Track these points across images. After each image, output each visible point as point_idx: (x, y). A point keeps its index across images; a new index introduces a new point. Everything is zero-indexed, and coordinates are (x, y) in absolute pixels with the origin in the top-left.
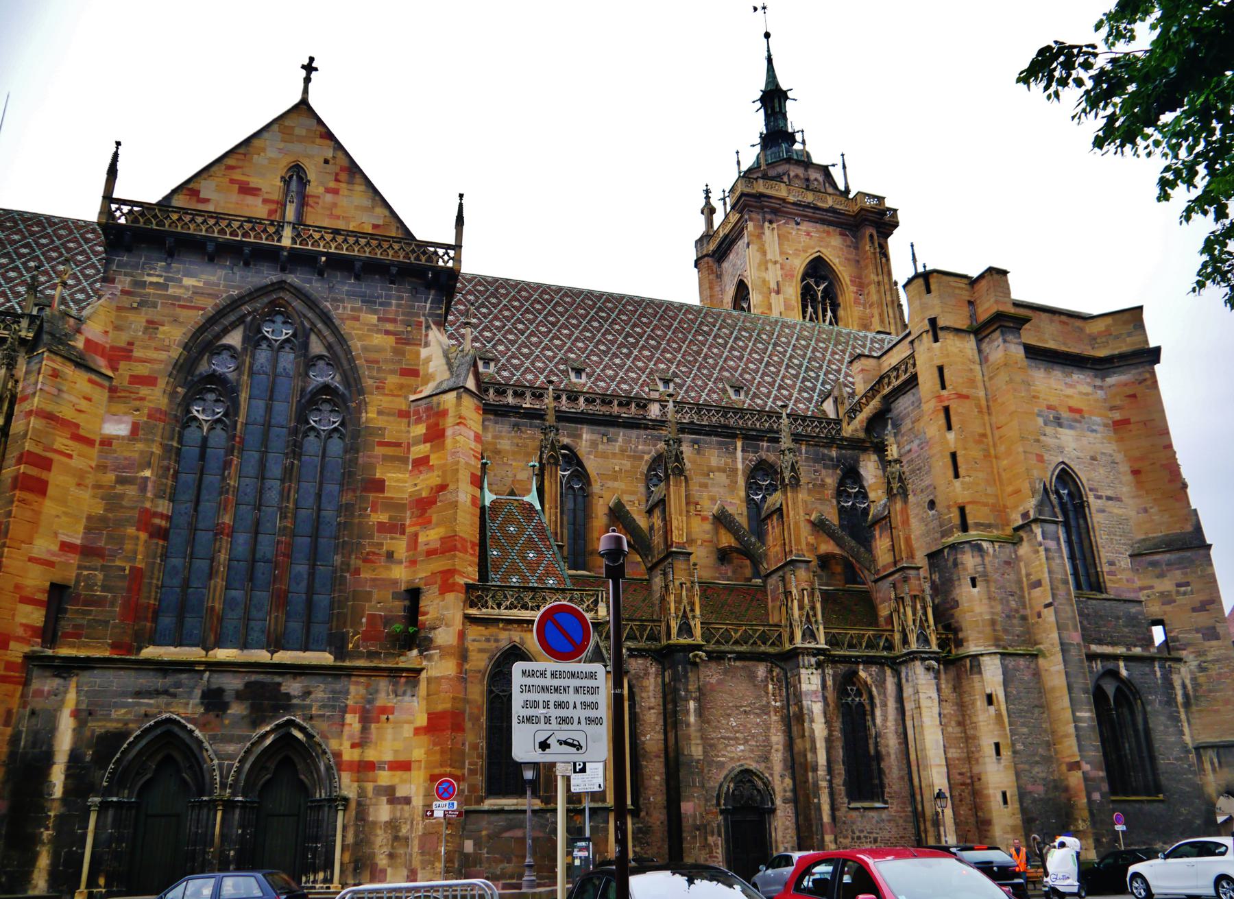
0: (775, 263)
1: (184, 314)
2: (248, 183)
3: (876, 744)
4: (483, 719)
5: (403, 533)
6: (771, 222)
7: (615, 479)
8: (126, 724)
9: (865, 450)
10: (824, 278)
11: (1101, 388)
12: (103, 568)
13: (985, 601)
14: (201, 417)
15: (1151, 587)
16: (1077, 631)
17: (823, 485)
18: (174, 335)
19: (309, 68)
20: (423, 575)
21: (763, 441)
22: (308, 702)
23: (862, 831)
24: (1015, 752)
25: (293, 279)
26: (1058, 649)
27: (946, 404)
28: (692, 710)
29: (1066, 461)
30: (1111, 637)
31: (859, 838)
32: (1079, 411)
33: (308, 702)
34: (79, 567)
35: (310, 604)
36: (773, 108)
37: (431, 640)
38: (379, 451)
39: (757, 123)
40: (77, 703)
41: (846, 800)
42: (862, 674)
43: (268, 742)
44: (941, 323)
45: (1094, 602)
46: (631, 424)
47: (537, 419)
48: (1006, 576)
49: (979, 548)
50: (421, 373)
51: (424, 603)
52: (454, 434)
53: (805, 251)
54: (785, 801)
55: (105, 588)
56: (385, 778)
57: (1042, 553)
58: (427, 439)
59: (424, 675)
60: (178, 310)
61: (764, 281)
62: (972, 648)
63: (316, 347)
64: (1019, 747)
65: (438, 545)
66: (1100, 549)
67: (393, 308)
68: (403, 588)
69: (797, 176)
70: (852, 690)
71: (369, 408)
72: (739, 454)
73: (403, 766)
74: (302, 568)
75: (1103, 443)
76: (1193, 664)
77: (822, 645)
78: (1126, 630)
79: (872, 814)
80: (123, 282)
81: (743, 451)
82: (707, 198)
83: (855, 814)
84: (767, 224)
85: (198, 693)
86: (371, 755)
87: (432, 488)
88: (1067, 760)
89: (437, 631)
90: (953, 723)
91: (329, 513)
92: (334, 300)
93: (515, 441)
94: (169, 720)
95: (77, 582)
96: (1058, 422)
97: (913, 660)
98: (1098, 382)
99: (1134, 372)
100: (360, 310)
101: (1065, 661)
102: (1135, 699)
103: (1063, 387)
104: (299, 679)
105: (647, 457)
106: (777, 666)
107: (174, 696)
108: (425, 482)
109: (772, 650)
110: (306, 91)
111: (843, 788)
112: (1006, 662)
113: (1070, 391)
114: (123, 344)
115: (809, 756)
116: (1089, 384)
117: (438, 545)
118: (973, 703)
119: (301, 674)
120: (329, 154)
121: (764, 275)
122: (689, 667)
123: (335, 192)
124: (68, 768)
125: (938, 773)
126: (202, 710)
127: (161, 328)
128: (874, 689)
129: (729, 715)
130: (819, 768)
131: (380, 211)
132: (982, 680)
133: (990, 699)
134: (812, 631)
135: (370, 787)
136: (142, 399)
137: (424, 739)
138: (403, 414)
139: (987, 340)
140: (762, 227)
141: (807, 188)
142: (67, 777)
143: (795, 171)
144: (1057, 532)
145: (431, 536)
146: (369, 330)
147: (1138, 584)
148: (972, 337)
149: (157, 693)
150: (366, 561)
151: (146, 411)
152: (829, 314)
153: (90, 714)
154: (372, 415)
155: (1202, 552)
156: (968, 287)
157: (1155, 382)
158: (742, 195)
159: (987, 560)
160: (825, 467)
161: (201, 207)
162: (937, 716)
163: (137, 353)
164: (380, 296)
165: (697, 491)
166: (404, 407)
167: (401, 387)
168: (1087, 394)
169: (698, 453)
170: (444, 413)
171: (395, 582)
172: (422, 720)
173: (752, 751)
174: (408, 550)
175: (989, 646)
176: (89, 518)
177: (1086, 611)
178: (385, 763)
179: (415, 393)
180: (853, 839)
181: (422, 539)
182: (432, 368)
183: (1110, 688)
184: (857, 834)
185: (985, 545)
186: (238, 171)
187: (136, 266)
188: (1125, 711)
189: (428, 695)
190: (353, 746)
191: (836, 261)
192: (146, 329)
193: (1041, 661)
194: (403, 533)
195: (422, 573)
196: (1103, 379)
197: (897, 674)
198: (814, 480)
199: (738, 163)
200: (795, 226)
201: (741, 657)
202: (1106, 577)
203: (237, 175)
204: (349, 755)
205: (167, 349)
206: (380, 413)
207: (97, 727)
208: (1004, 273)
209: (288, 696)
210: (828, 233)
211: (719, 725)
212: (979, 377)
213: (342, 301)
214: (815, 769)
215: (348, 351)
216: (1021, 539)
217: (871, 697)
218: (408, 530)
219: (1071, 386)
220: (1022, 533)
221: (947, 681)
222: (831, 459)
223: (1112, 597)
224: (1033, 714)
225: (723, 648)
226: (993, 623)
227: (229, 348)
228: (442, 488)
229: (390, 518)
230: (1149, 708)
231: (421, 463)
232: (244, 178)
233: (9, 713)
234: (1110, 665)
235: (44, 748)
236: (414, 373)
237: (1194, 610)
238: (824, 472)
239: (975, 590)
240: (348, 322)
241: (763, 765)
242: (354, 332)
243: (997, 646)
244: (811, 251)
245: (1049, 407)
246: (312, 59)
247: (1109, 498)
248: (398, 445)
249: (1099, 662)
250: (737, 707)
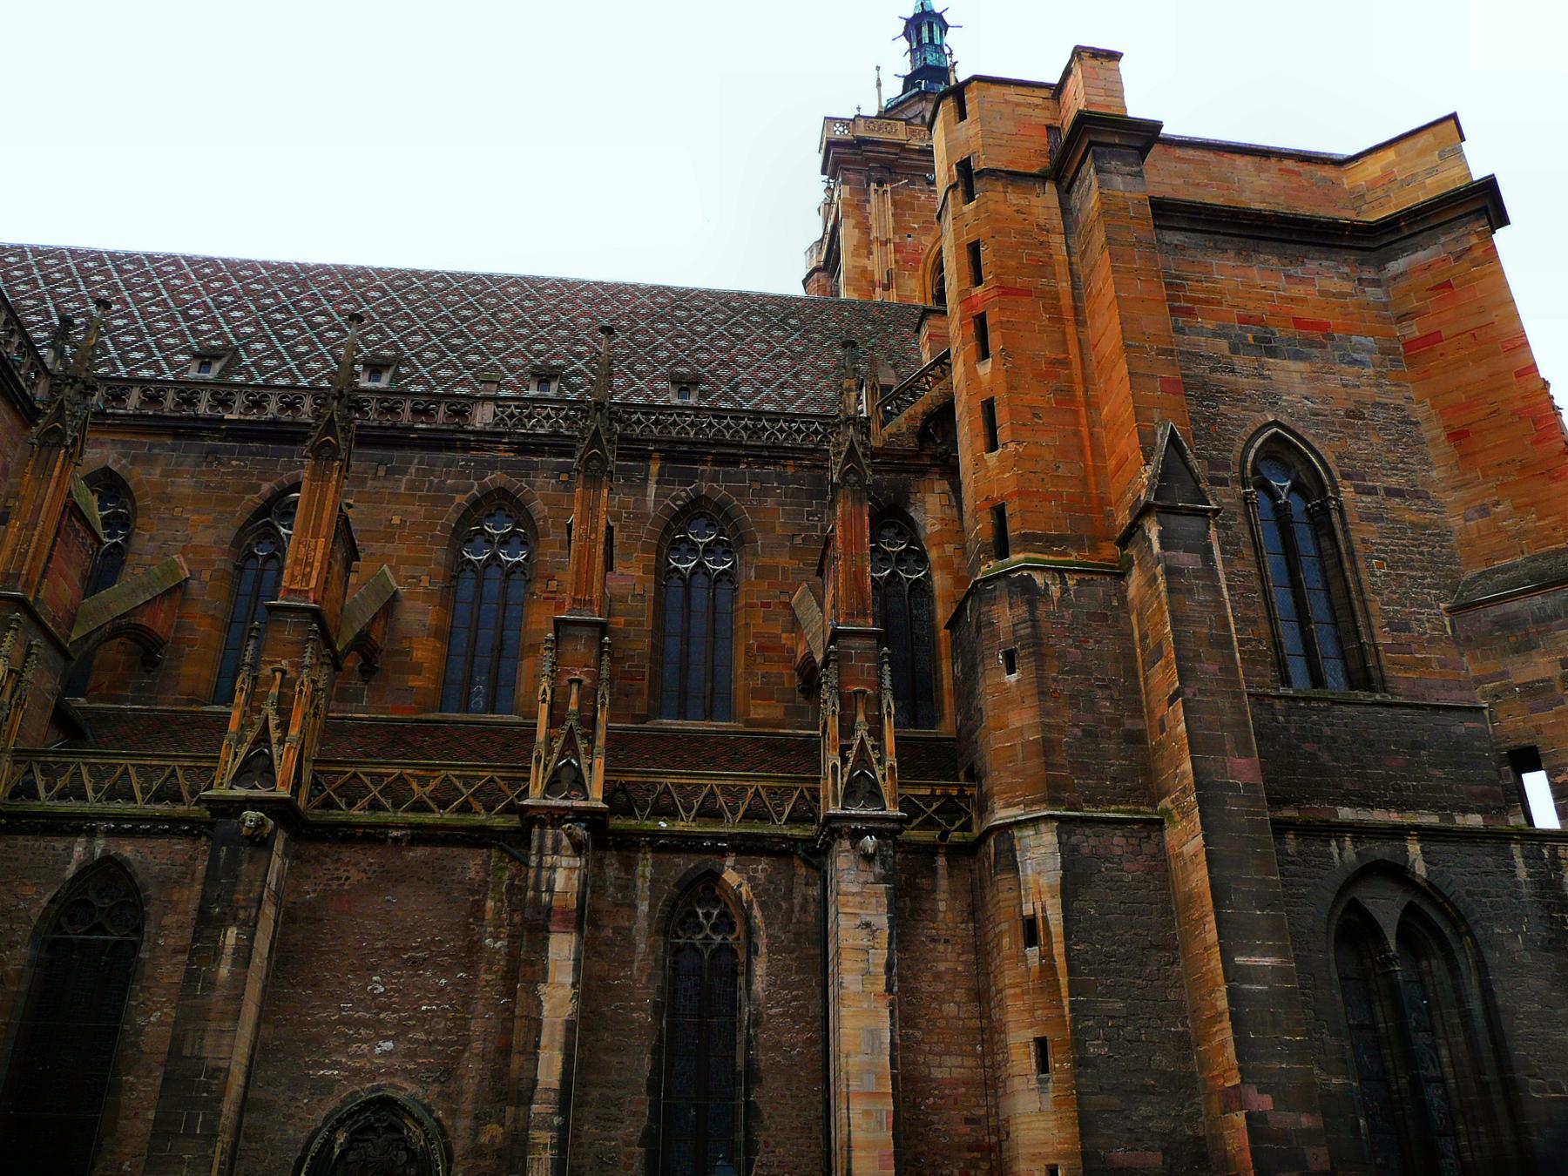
0: (885, 243)
6: (880, 183)
7: (390, 538)
9: (922, 472)
11: (1376, 283)
13: (1032, 701)
15: (1504, 674)
16: (1249, 755)
21: (705, 463)
24: (1082, 1063)
28: (229, 950)
29: (1284, 419)
30: (1398, 790)
32: (1322, 327)
36: (919, 41)
42: (731, 877)
44: (977, 166)
45: (1347, 710)
46: (436, 442)
47: (253, 440)
48: (1091, 644)
49: (1027, 587)
61: (864, 270)
64: (1095, 1049)
66: (1369, 596)
70: (708, 916)
72: (652, 489)
75: (1379, 385)
78: (1438, 773)
81: (658, 482)
84: (873, 186)
90: (960, 994)
93: (204, 478)
96: (1267, 346)
98: (1369, 273)
102: (1460, 936)
103: (1283, 282)
105: (459, 499)
111: (639, 1151)
112: (1074, 840)
113: (1298, 291)
116: (1345, 277)
121: (865, 262)
122: (245, 851)
125: (867, 1114)
128: (756, 912)
129: (373, 969)
130: (537, 1096)
134: (579, 771)
140: (866, 192)
144: (1206, 535)
148: (1050, 187)
156: (1050, 103)
159: (1041, 610)
162: (882, 970)
165: (554, 555)
168: (1342, 295)
173: (411, 1055)
175: (1033, 803)
177: (1327, 730)
183: (1386, 908)
185: (1039, 579)
188: (1437, 965)
196: (1381, 265)
198: (807, 528)
200: (926, 187)
201: (423, 836)
202: (1386, 657)
211: (339, 990)
212: (1061, 255)
217: (750, 932)
219: (1301, 281)
221: (954, 894)
223: (1400, 699)
224: (1143, 965)
225: (382, 816)
230: (1493, 957)
234: (1381, 850)
239: (1013, 678)
241: (436, 1088)
243: (1053, 801)
245: (1243, 320)
247: (1391, 492)
249: (1348, 843)
250: (395, 952)
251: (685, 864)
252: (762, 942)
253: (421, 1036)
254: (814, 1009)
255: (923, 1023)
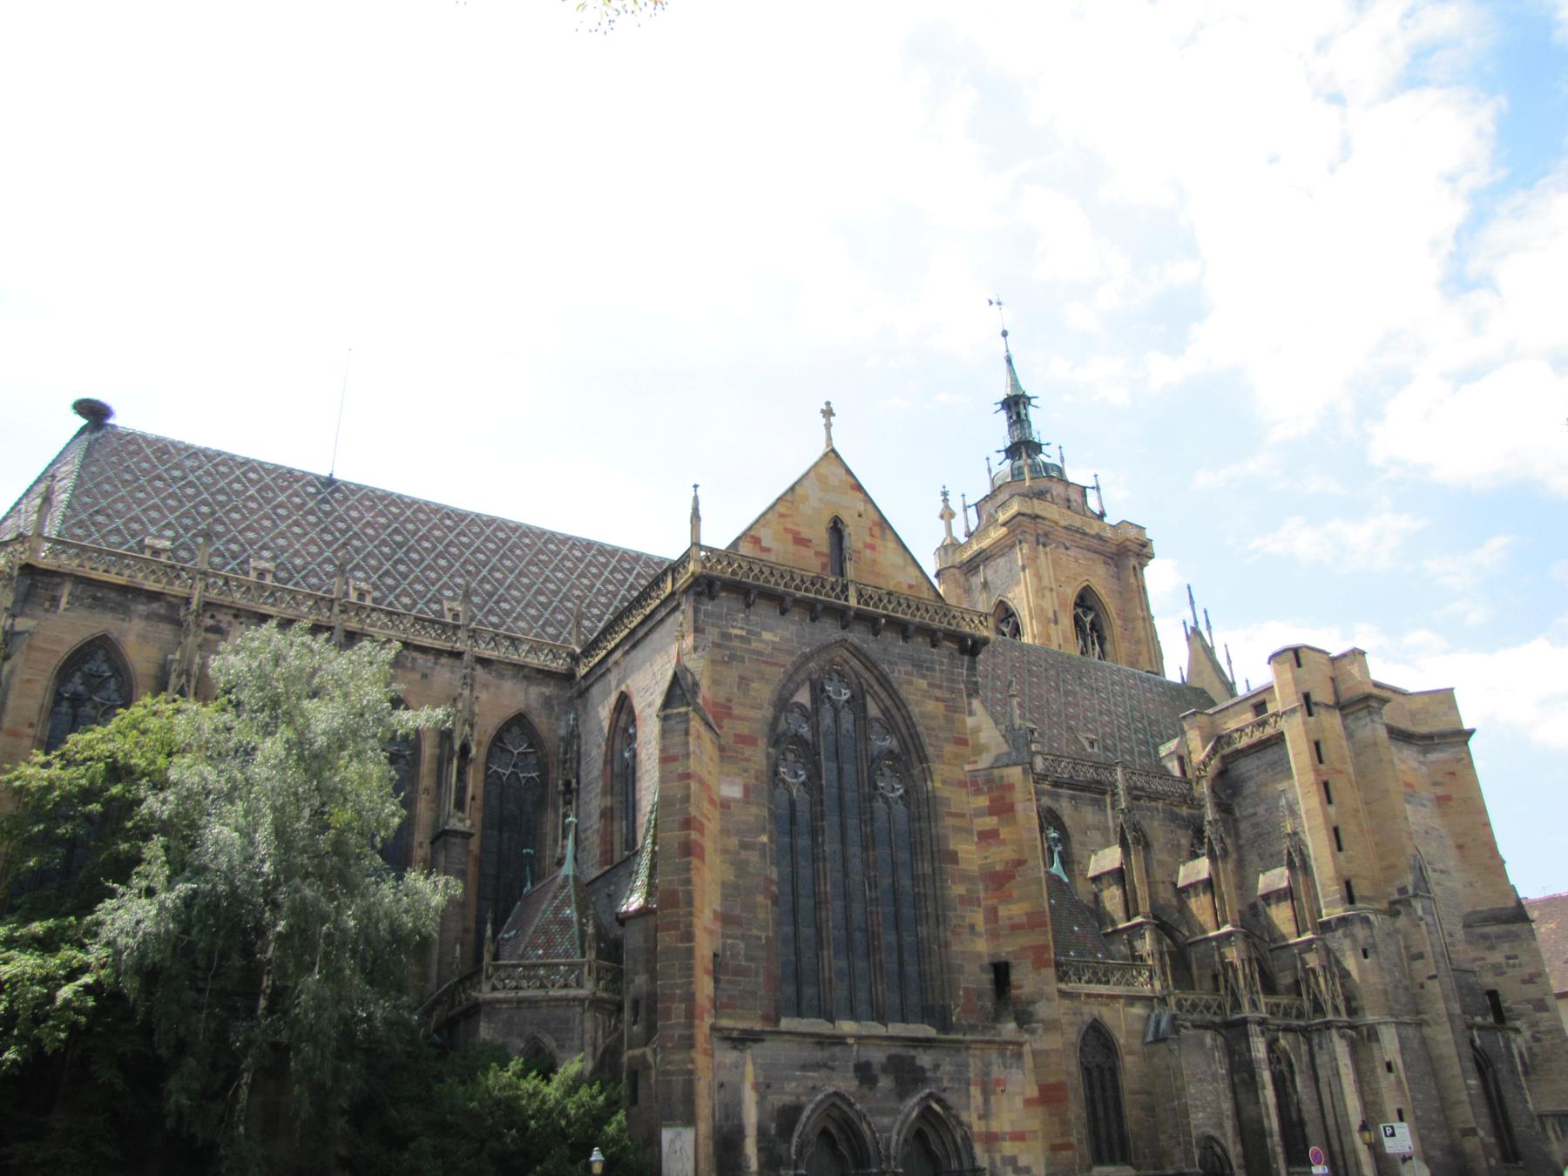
1: (768, 670)
2: (799, 533)
3: (1299, 1111)
4: (1081, 1090)
5: (979, 906)
8: (798, 1098)
10: (1090, 609)
12: (743, 937)
14: (789, 779)
15: (1483, 959)
17: (1179, 846)
18: (764, 692)
19: (828, 413)
20: (1010, 949)
22: (939, 1074)
24: (1417, 1118)
25: (857, 636)
26: (1445, 1019)
27: (1325, 778)
33: (939, 1074)
34: (724, 936)
35: (902, 975)
37: (1031, 1014)
38: (950, 822)
39: (999, 432)
40: (756, 1076)
42: (1282, 1042)
43: (914, 1114)
44: (1315, 698)
49: (1366, 921)
50: (970, 742)
51: (1015, 977)
52: (1025, 809)
53: (1075, 579)
54: (1239, 1167)
55: (749, 958)
56: (1008, 1148)
57: (1424, 927)
58: (992, 811)
59: (1027, 1048)
60: (763, 666)
61: (1042, 609)
62: (1370, 1018)
63: (873, 710)
64: (1419, 1113)
65: (1024, 919)
67: (938, 674)
68: (986, 961)
69: (1058, 495)
71: (935, 778)
73: (1019, 1136)
74: (890, 938)
76: (1527, 1034)
77: (1264, 1014)
80: (712, 634)
82: (945, 500)
85: (851, 1064)
86: (995, 1126)
87: (1007, 863)
88: (1461, 1126)
89: (1037, 1006)
91: (906, 882)
92: (890, 663)
94: (836, 1094)
95: (724, 950)
97: (1328, 1028)
98: (1422, 759)
99: (1451, 750)
100: (911, 674)
101: (1453, 1031)
104: (931, 1051)
106: (1220, 1033)
107: (832, 1069)
108: (999, 856)
109: (1217, 1019)
110: (829, 438)
114: (722, 701)
115: (1266, 1121)
117: (1024, 919)
118: (1373, 1071)
119: (930, 1047)
120: (861, 506)
123: (872, 547)
124: (759, 1141)
126: (856, 1083)
127: (754, 685)
131: (912, 570)
132: (1380, 1049)
133: (1389, 1067)
135: (998, 1157)
136: (748, 760)
137: (1039, 1110)
138: (962, 784)
139: (1352, 717)
141: (1069, 508)
142: (759, 1150)
143: (1057, 489)
145: (1014, 911)
146: (923, 696)
147: (1473, 954)
148: (1337, 712)
149: (818, 1066)
150: (954, 933)
151: (753, 773)
152: (1097, 647)
153: (768, 1087)
154: (938, 784)
155: (1526, 926)
157: (1471, 762)
158: (1019, 514)
160: (1179, 827)
161: (764, 556)
163: (737, 711)
164: (925, 661)
166: (962, 778)
167: (957, 756)
168: (1415, 770)
169: (1076, 809)
170: (1011, 787)
171: (979, 956)
172: (1033, 1091)
173: (1209, 1118)
174: (987, 921)
176: (723, 884)
178: (1005, 1133)
179: (969, 763)
181: (1003, 912)
182: (983, 737)
185: (1372, 917)
186: (789, 519)
187: (719, 617)
189: (1035, 1067)
190: (980, 1118)
191: (1103, 592)
192: (740, 684)
193: (1426, 1030)
194: (979, 906)
195: (1007, 949)
197: (1309, 1042)
199: (990, 470)
203: (790, 526)
204: (978, 1127)
205: (760, 707)
206: (944, 782)
207: (777, 1100)
208: (1363, 653)
209: (922, 1069)
210: (1093, 560)
213: (895, 664)
214: (1272, 1136)
215: (908, 718)
216: (1398, 913)
217: (1290, 1065)
218: (983, 903)
220: (1399, 907)
222: (1183, 819)
226: (1386, 993)
227: (801, 706)
228: (1020, 863)
229: (967, 890)
230: (1499, 1076)
231: (988, 836)
232: (795, 528)
235: (736, 1122)
236: (962, 742)
237: (1524, 982)
238: (1179, 832)
239: (1367, 961)
240: (905, 686)
242: (911, 697)
243: (1392, 1015)
244: (1081, 579)
246: (828, 404)
247: (1442, 872)
248: (962, 816)
252: (1296, 1068)
254: (1315, 1097)
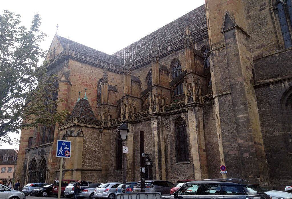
23: (181, 172)
31: (180, 174)
41: (176, 161)
70: (182, 122)
79: (184, 165)
83: (178, 166)
173: (149, 148)
180: (178, 175)
184: (179, 173)
233: (23, 159)
251: (176, 116)
253: (150, 145)
255: (212, 133)
